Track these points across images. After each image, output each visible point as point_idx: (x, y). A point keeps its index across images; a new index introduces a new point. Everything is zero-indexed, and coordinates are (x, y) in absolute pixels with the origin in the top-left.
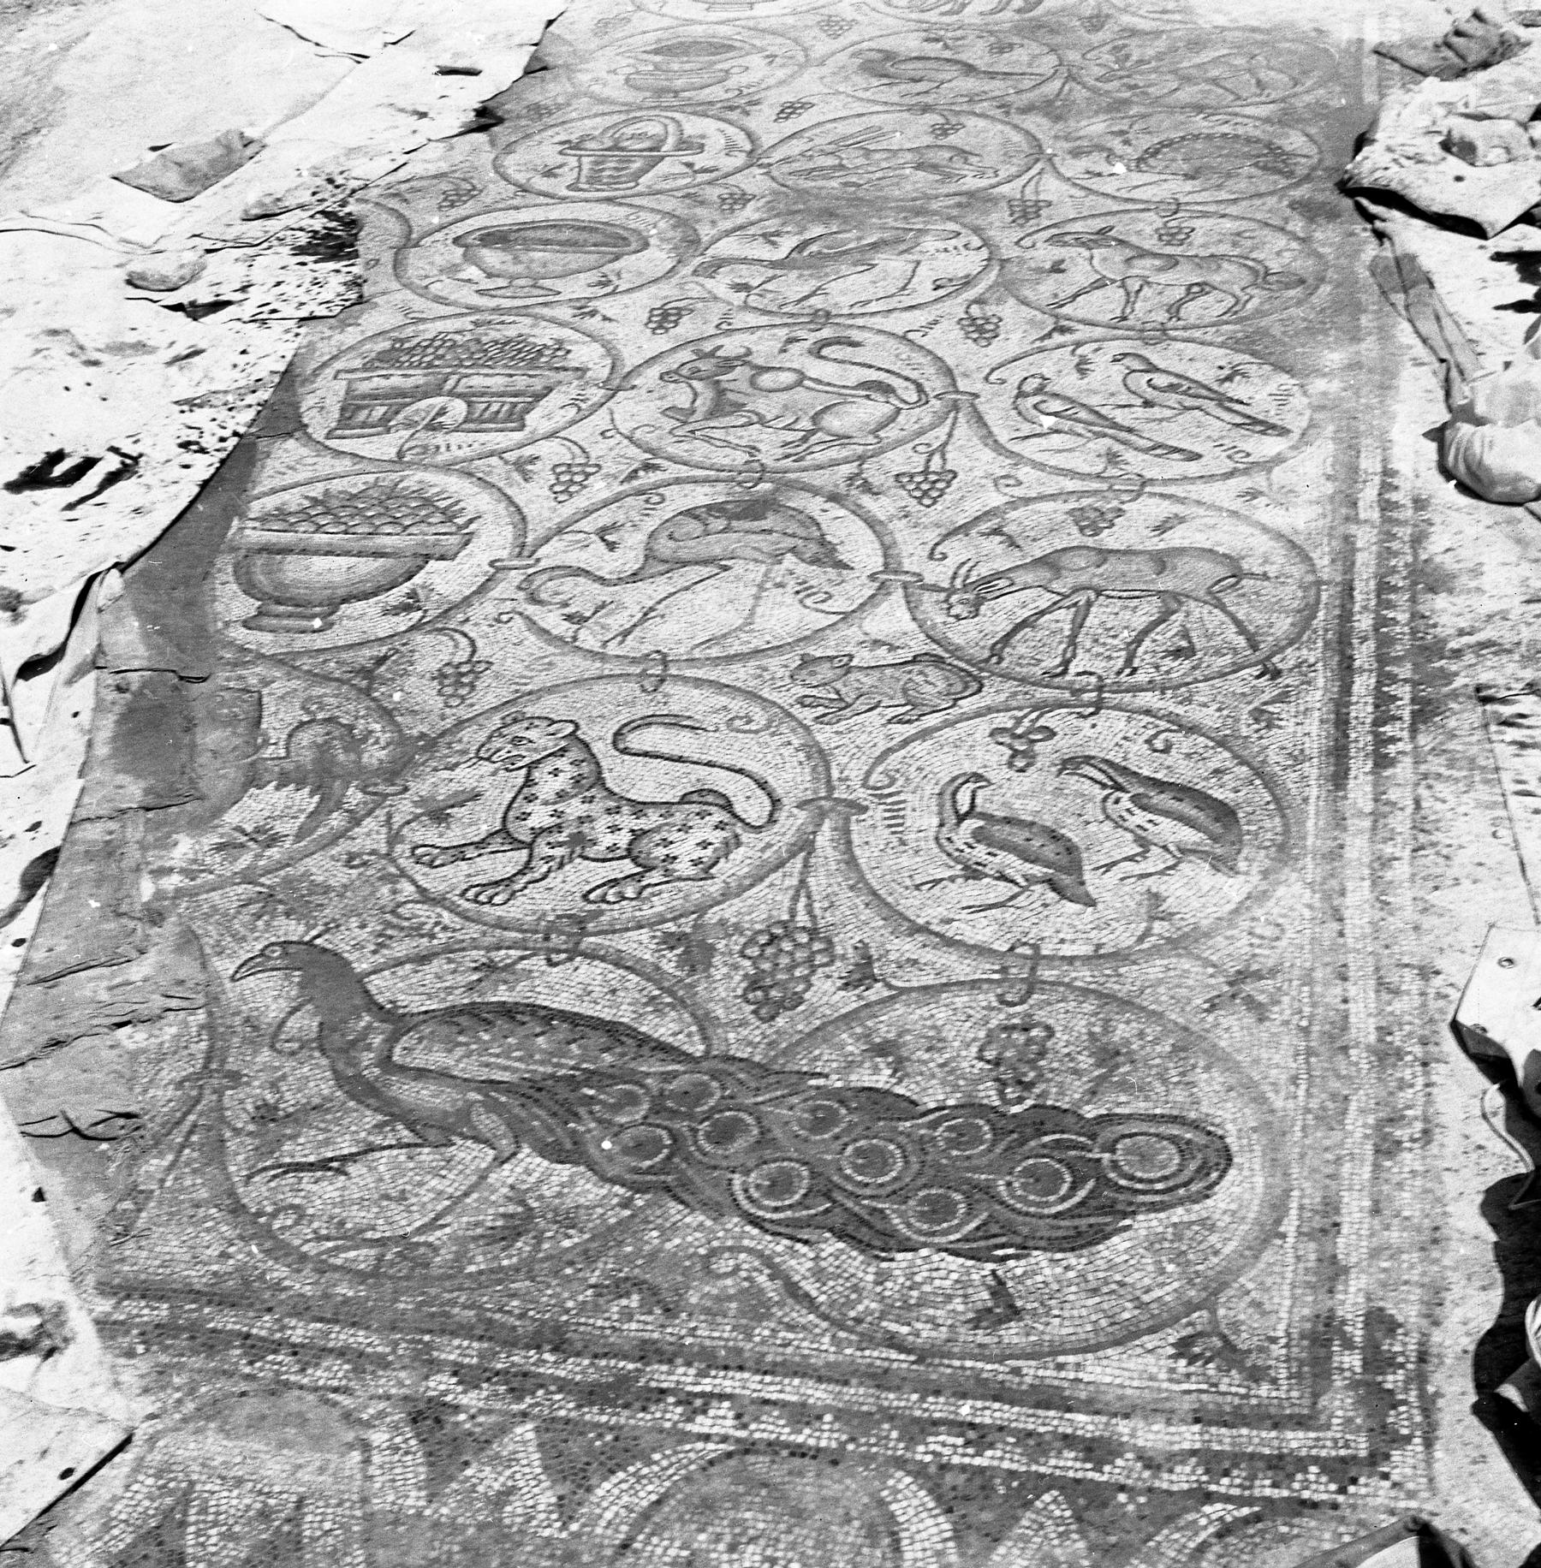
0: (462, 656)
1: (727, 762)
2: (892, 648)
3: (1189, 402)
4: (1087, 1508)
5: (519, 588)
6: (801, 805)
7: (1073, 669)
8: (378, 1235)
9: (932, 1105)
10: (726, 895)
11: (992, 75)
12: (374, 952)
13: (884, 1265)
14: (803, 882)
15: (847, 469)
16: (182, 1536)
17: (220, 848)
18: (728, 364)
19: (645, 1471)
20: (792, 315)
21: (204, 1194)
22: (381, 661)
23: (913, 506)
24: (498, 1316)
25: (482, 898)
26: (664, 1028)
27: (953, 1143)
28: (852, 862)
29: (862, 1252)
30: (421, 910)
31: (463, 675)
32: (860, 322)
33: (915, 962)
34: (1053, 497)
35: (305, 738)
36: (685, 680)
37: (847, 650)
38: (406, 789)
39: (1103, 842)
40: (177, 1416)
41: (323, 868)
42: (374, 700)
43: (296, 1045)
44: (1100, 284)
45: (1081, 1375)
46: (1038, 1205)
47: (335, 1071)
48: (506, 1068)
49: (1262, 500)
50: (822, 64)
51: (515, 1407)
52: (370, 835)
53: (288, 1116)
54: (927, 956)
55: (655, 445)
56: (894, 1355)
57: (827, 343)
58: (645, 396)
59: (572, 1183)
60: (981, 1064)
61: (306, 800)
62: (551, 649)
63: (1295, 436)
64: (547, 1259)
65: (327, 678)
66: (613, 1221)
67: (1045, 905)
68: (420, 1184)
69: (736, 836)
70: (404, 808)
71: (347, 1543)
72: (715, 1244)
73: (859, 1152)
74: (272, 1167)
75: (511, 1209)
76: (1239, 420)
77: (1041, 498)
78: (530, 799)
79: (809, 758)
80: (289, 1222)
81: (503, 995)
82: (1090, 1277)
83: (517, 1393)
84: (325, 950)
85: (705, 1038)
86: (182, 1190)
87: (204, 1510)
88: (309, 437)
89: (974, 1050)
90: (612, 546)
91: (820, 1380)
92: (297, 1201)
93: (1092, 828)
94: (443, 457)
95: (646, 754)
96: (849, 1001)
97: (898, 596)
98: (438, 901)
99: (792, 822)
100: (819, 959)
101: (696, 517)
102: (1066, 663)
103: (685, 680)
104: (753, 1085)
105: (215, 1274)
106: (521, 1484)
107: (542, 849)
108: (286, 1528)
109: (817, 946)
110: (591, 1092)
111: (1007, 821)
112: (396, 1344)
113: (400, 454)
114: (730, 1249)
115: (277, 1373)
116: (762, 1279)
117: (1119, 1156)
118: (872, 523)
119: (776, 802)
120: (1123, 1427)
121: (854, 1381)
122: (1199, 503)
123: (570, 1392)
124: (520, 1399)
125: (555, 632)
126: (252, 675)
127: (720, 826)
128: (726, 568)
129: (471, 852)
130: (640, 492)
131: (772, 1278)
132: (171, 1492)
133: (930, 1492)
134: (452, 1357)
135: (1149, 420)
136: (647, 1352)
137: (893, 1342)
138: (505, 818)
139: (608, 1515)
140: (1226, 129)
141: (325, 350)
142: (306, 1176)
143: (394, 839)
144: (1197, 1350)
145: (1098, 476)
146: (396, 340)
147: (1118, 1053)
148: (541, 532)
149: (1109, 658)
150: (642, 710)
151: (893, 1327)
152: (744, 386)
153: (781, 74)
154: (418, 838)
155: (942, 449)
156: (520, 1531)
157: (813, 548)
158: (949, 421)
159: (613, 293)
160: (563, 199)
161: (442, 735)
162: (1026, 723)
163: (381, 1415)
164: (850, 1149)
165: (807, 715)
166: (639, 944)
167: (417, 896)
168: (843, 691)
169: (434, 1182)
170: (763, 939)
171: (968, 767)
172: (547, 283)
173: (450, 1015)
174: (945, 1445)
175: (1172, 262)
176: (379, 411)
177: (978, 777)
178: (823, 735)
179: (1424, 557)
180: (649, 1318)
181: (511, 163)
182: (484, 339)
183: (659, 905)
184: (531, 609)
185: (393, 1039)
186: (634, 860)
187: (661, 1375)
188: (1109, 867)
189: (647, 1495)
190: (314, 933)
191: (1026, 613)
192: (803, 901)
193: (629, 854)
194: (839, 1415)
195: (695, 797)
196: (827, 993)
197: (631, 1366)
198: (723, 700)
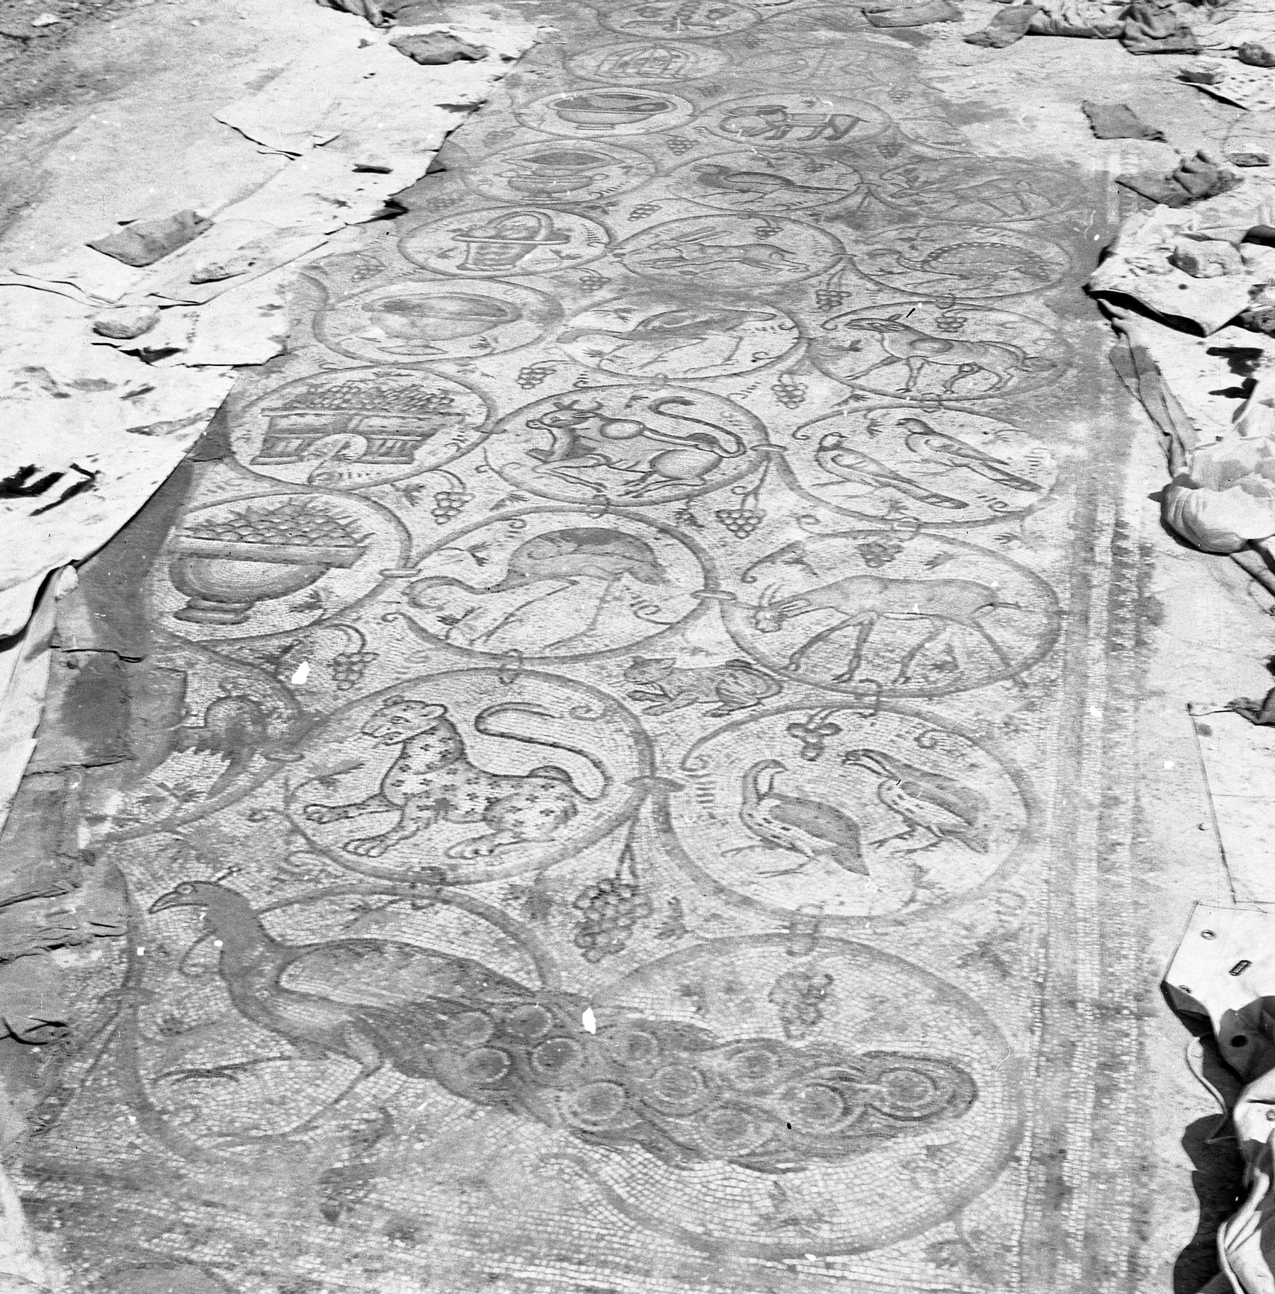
0: (354, 648)
1: (569, 744)
2: (708, 654)
3: (959, 460)
5: (404, 594)
7: (857, 677)
8: (261, 1133)
9: (730, 1038)
10: (564, 855)
11: (806, 189)
12: (269, 893)
13: (685, 1173)
14: (628, 847)
15: (680, 505)
17: (146, 801)
18: (582, 416)
20: (635, 377)
21: (117, 1093)
22: (287, 650)
25: (361, 851)
26: (507, 967)
30: (308, 858)
31: (353, 663)
32: (691, 385)
34: (845, 534)
35: (221, 711)
38: (302, 757)
40: (85, 1283)
41: (231, 822)
42: (280, 681)
44: (890, 361)
45: (846, 1274)
47: (231, 992)
48: (374, 995)
49: (1015, 543)
50: (667, 175)
52: (269, 796)
53: (191, 1029)
54: (730, 912)
55: (520, 479)
57: (665, 401)
58: (512, 436)
61: (218, 764)
62: (428, 645)
63: (1045, 491)
65: (242, 663)
68: (298, 1092)
69: (574, 806)
70: (299, 773)
74: (176, 1073)
75: (373, 1115)
76: (999, 476)
77: (835, 535)
78: (403, 770)
79: (636, 743)
80: (188, 1120)
84: (229, 890)
85: (542, 976)
86: (100, 1089)
90: (481, 562)
92: (196, 1102)
93: (869, 809)
95: (502, 735)
97: (715, 610)
98: (325, 852)
99: (620, 796)
100: (640, 911)
101: (552, 540)
102: (851, 672)
107: (412, 811)
109: (637, 900)
111: (798, 801)
113: (310, 479)
114: (556, 1156)
118: (695, 550)
119: (608, 779)
122: (964, 544)
125: (431, 631)
128: (574, 583)
129: (353, 812)
134: (318, 1241)
135: (925, 474)
138: (382, 785)
140: (995, 240)
141: (254, 391)
143: (289, 799)
144: (944, 1255)
145: (883, 519)
146: (312, 386)
148: (423, 548)
149: (888, 669)
152: (594, 433)
153: (635, 182)
155: (755, 492)
157: (646, 570)
158: (762, 469)
159: (491, 354)
160: (454, 276)
162: (817, 720)
165: (637, 708)
166: (490, 893)
167: (306, 847)
168: (667, 687)
169: (310, 1090)
170: (592, 894)
171: (768, 755)
172: (438, 344)
175: (948, 346)
176: (295, 443)
177: (777, 763)
178: (649, 724)
181: (412, 245)
182: (384, 388)
184: (412, 612)
188: (881, 843)
190: (220, 875)
191: (821, 629)
196: (644, 942)
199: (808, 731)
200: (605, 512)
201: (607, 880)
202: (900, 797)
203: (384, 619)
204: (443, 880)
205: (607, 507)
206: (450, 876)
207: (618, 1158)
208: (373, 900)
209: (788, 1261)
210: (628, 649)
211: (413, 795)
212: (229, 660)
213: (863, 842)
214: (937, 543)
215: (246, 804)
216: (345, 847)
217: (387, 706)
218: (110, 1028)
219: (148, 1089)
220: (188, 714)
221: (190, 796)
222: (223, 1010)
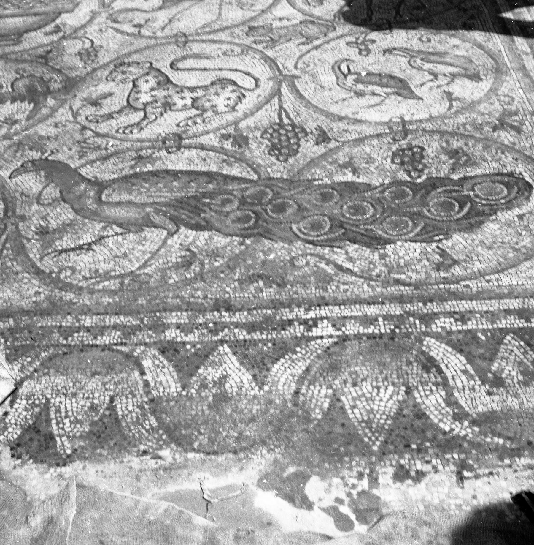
0: (88, 44)
6: (270, 79)
8: (118, 273)
14: (281, 107)
16: (50, 425)
19: (294, 357)
21: (19, 268)
26: (235, 171)
27: (393, 199)
28: (301, 96)
30: (99, 140)
35: (20, 84)
40: (31, 369)
41: (43, 130)
47: (73, 209)
48: (161, 196)
51: (215, 338)
54: (351, 128)
56: (402, 288)
59: (210, 238)
60: (394, 165)
61: (28, 107)
64: (209, 271)
68: (133, 249)
71: (144, 415)
73: (349, 207)
75: (183, 253)
78: (138, 92)
79: (265, 61)
81: (149, 168)
82: (486, 242)
83: (214, 332)
85: (256, 172)
87: (58, 411)
89: (389, 160)
91: (369, 304)
92: (70, 265)
95: (188, 69)
96: (321, 150)
103: (197, 41)
105: (34, 302)
108: (107, 413)
110: (208, 201)
116: (323, 265)
117: (477, 192)
119: (256, 80)
121: (387, 302)
123: (242, 327)
124: (217, 334)
127: (234, 91)
131: (327, 264)
133: (447, 344)
134: (174, 321)
136: (277, 305)
138: (128, 101)
139: (283, 380)
142: (72, 254)
143: (75, 115)
151: (397, 276)
156: (237, 394)
161: (88, 74)
162: (361, 38)
163: (143, 352)
164: (345, 207)
165: (260, 47)
173: (126, 179)
178: (270, 53)
180: (272, 290)
183: (215, 125)
184: (115, 25)
185: (99, 193)
186: (197, 109)
187: (286, 314)
189: (300, 368)
190: (46, 155)
192: (284, 115)
193: (193, 106)
194: (385, 318)
196: (309, 149)
197: (269, 312)
198: (217, 46)
201: (276, 124)
207: (339, 250)
208: (143, 153)
209: (463, 283)
210: (243, 23)
211: (148, 103)
212: (16, 61)
213: (412, 87)
215: (50, 121)
216: (117, 131)
219: (38, 264)
221: (15, 122)
222: (71, 217)
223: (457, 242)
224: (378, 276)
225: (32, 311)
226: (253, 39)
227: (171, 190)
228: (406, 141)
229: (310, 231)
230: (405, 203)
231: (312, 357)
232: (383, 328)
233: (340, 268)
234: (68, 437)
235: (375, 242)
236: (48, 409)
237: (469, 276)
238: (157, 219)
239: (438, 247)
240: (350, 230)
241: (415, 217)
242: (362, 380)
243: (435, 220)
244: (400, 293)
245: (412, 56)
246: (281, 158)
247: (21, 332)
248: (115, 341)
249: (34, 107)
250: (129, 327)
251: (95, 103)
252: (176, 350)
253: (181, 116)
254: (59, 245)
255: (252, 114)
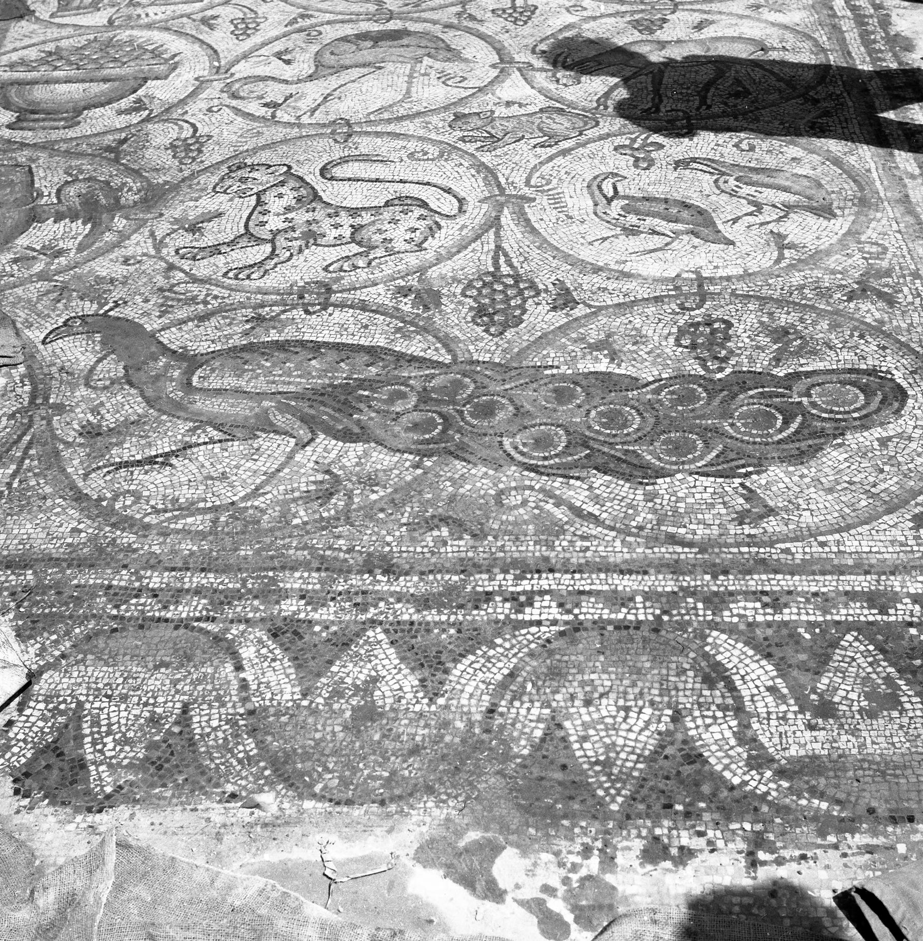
0: (187, 132)
1: (416, 179)
2: (520, 105)
4: (886, 641)
5: (222, 91)
7: (663, 110)
8: (209, 505)
9: (651, 379)
10: (439, 260)
14: (498, 247)
16: (81, 746)
17: (15, 261)
19: (491, 653)
21: (48, 490)
23: (510, 26)
24: (328, 553)
26: (415, 347)
28: (534, 231)
29: (627, 480)
30: (194, 288)
33: (605, 289)
35: (72, 191)
36: (367, 133)
37: (489, 108)
38: (161, 215)
39: (724, 209)
40: (57, 653)
41: (104, 267)
43: (108, 383)
45: (842, 548)
46: (761, 436)
47: (144, 397)
48: (289, 383)
54: (611, 285)
56: (679, 549)
60: (680, 349)
61: (81, 229)
66: (409, 478)
67: (695, 247)
68: (237, 467)
69: (436, 223)
72: (501, 486)
74: (105, 466)
75: (320, 477)
78: (264, 213)
79: (478, 172)
80: (128, 503)
81: (274, 336)
82: (823, 480)
83: (362, 607)
84: (119, 318)
85: (449, 351)
86: (29, 488)
87: (96, 723)
88: (37, 19)
89: (671, 340)
90: (288, 62)
91: (622, 572)
92: (133, 487)
93: (713, 198)
94: (144, 20)
95: (349, 179)
99: (477, 213)
103: (367, 133)
104: (499, 378)
105: (69, 545)
106: (384, 673)
108: (176, 729)
110: (366, 393)
112: (244, 581)
113: (111, 22)
115: (143, 612)
116: (549, 507)
117: (815, 398)
118: (482, 37)
119: (461, 201)
120: (896, 583)
121: (652, 571)
122: (720, 13)
123: (408, 601)
124: (365, 610)
125: (257, 114)
126: (22, 157)
127: (422, 218)
128: (380, 68)
130: (300, 30)
131: (557, 505)
132: (62, 713)
133: (746, 644)
134: (296, 586)
136: (466, 567)
137: (673, 539)
138: (246, 226)
139: (469, 689)
142: (136, 470)
143: (159, 245)
147: (788, 333)
148: (230, 58)
149: (688, 101)
150: (337, 155)
151: (671, 530)
154: (180, 243)
156: (393, 710)
161: (183, 180)
164: (593, 413)
165: (471, 148)
166: (380, 295)
168: (493, 132)
169: (248, 464)
173: (235, 352)
174: (750, 610)
178: (486, 158)
179: (893, 33)
180: (462, 543)
184: (234, 103)
185: (190, 372)
186: (359, 244)
190: (106, 308)
192: (502, 260)
193: (353, 240)
195: (396, 202)
196: (540, 316)
197: (455, 578)
198: (401, 143)
199: (632, 149)
200: (391, 18)
202: (737, 186)
203: (210, 110)
204: (329, 290)
205: (391, 16)
206: (335, 287)
207: (578, 483)
210: (446, 108)
211: (279, 231)
213: (719, 223)
214: (696, 14)
215: (117, 253)
216: (225, 275)
217: (231, 171)
218: (27, 438)
219: (80, 484)
220: (40, 195)
221: (60, 253)
222: (140, 411)
223: (776, 480)
224: (641, 528)
225: (65, 560)
226: (459, 134)
227: (307, 374)
228: (703, 310)
229: (533, 450)
230: (693, 410)
231: (521, 655)
232: (643, 613)
233: (577, 512)
234: (110, 766)
235: (637, 472)
236: (80, 718)
237: (792, 535)
238: (280, 420)
239: (742, 485)
240: (599, 451)
241: (709, 434)
242: (602, 696)
243: (742, 441)
244: (675, 557)
245: (723, 174)
246: (492, 330)
247: (44, 593)
248: (197, 614)
249: (91, 230)
250: (221, 592)
251: (194, 229)
252: (296, 633)
253: (333, 254)
254: (117, 454)
255: (451, 256)
